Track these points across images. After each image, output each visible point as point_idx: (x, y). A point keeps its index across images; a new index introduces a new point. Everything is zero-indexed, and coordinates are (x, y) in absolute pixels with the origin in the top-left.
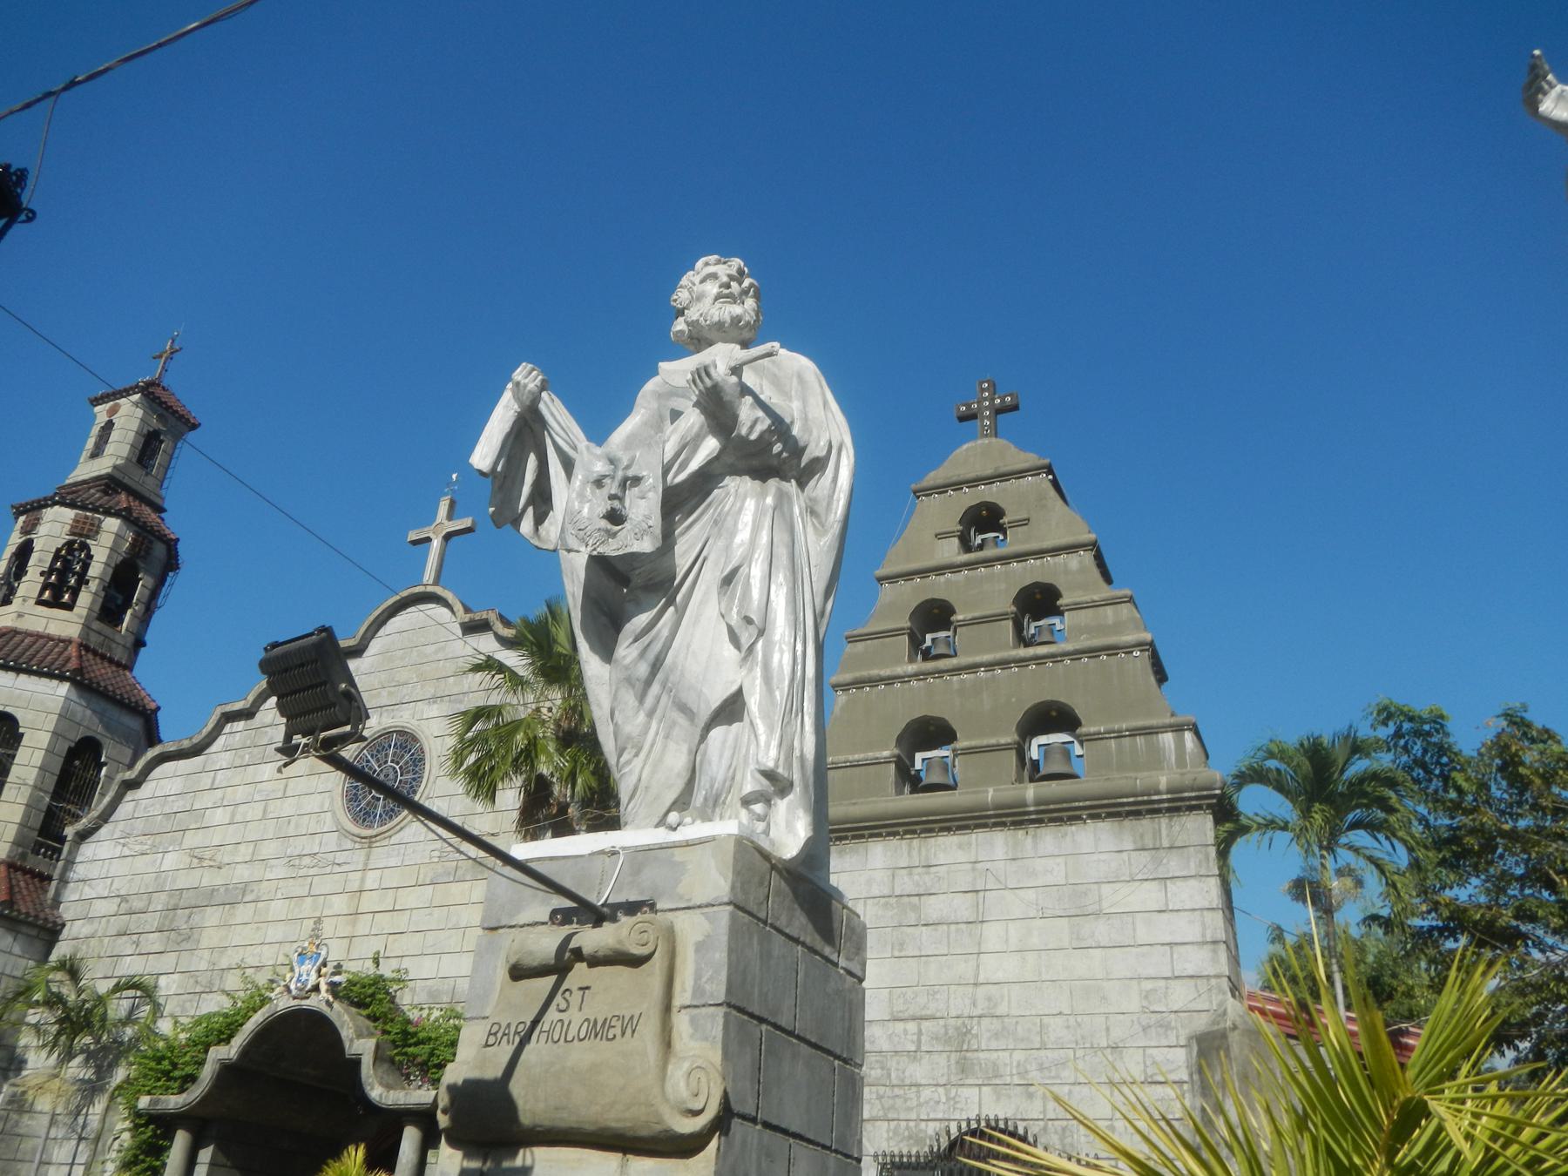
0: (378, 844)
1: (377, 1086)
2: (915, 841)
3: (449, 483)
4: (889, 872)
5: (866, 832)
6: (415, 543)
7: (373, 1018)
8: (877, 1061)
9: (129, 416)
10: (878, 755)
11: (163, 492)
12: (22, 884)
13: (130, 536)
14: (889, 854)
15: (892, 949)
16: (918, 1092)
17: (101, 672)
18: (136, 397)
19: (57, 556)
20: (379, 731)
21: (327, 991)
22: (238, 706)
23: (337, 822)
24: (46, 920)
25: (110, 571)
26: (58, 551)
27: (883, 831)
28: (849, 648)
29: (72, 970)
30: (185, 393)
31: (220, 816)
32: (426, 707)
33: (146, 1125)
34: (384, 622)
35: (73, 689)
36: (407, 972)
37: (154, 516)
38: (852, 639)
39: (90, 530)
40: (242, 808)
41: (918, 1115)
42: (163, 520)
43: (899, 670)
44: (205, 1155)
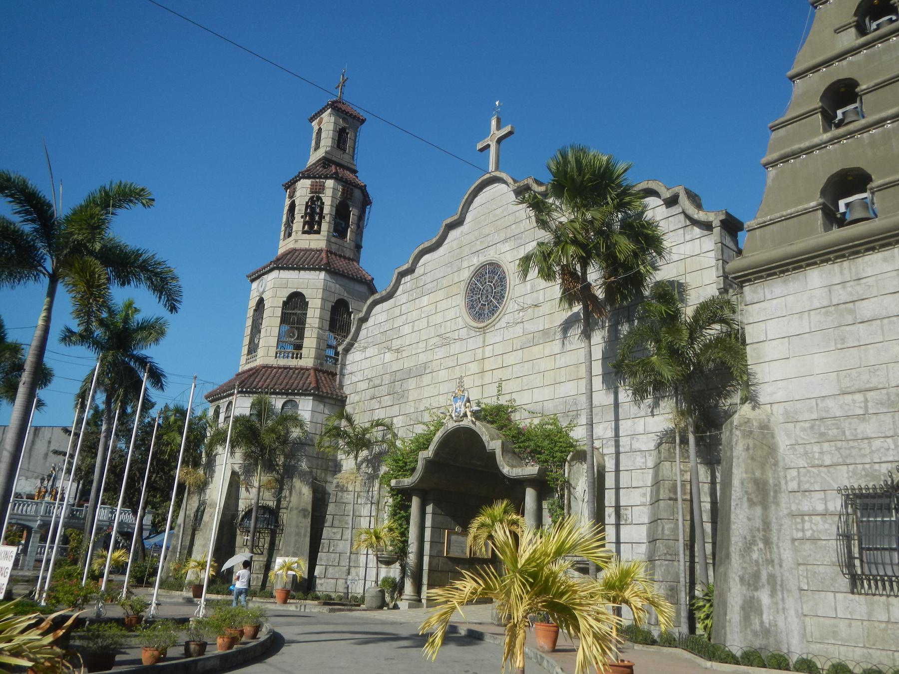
1: (505, 466)
2: (845, 263)
3: (495, 108)
4: (826, 289)
5: (803, 263)
6: (482, 150)
7: (500, 428)
8: (833, 424)
9: (328, 122)
10: (806, 206)
11: (355, 163)
12: (323, 378)
13: (340, 188)
14: (824, 276)
15: (836, 343)
16: (870, 443)
17: (340, 264)
18: (329, 110)
19: (307, 206)
21: (471, 416)
22: (405, 267)
23: (466, 323)
24: (337, 395)
25: (334, 209)
26: (307, 203)
27: (818, 260)
28: (774, 135)
29: (349, 419)
30: (356, 102)
31: (407, 329)
32: (502, 246)
33: (397, 495)
34: (472, 202)
35: (327, 275)
36: (515, 400)
37: (351, 175)
38: (774, 128)
39: (320, 189)
40: (416, 323)
41: (872, 460)
42: (357, 177)
43: (816, 140)
44: (429, 509)
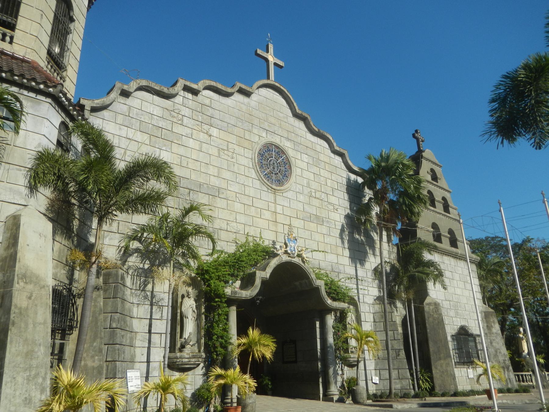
0: (278, 194)
20: (269, 142)
22: (194, 86)
31: (191, 143)
32: (285, 141)
